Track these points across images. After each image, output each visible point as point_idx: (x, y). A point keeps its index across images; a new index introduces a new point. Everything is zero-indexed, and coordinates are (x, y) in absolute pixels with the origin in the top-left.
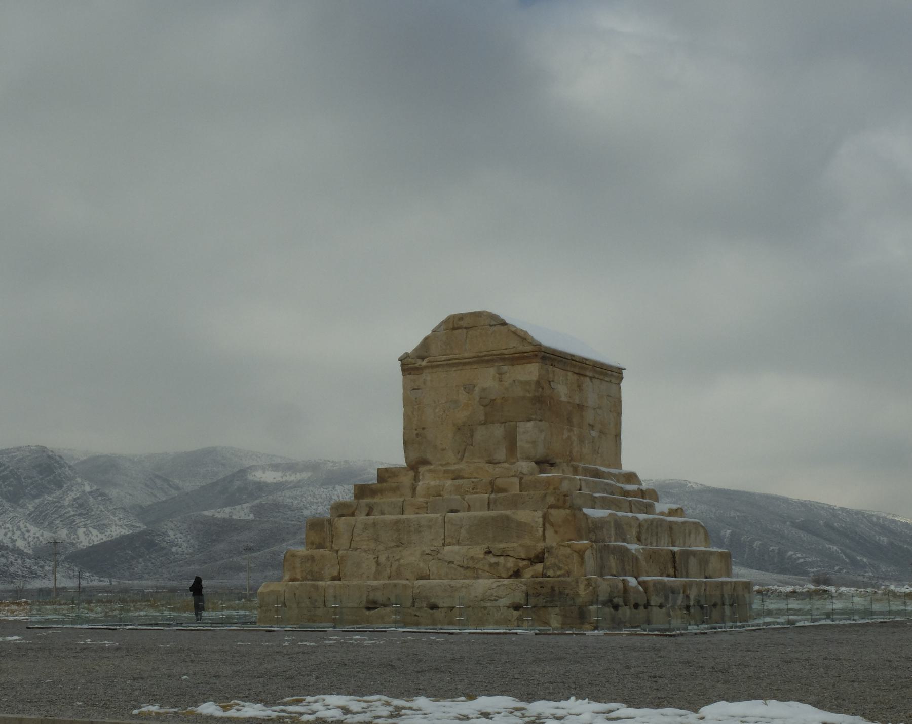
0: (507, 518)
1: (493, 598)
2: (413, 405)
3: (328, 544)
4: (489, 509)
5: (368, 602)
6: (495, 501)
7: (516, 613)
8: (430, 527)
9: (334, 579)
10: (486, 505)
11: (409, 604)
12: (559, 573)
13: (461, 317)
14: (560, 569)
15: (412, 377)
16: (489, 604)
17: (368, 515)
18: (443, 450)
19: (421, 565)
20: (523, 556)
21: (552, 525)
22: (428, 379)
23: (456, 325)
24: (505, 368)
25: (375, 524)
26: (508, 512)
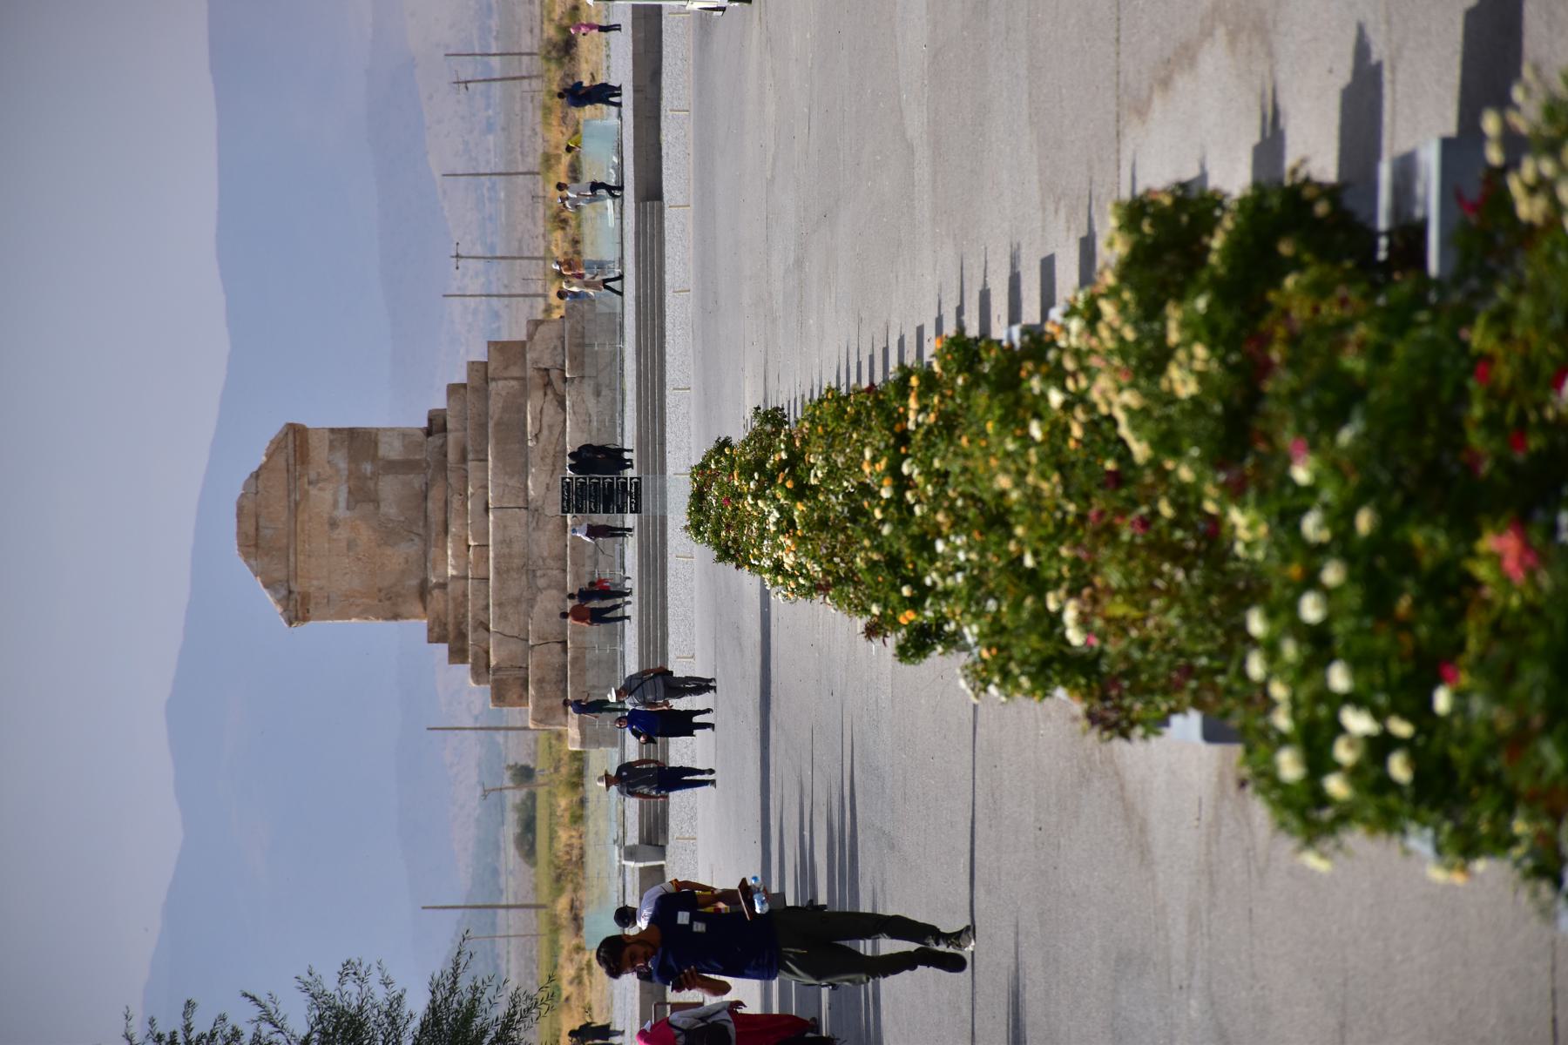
0: (497, 424)
2: (345, 607)
7: (605, 392)
9: (565, 650)
13: (241, 534)
15: (312, 607)
19: (550, 527)
21: (506, 368)
22: (315, 582)
23: (253, 543)
24: (313, 476)
25: (500, 605)
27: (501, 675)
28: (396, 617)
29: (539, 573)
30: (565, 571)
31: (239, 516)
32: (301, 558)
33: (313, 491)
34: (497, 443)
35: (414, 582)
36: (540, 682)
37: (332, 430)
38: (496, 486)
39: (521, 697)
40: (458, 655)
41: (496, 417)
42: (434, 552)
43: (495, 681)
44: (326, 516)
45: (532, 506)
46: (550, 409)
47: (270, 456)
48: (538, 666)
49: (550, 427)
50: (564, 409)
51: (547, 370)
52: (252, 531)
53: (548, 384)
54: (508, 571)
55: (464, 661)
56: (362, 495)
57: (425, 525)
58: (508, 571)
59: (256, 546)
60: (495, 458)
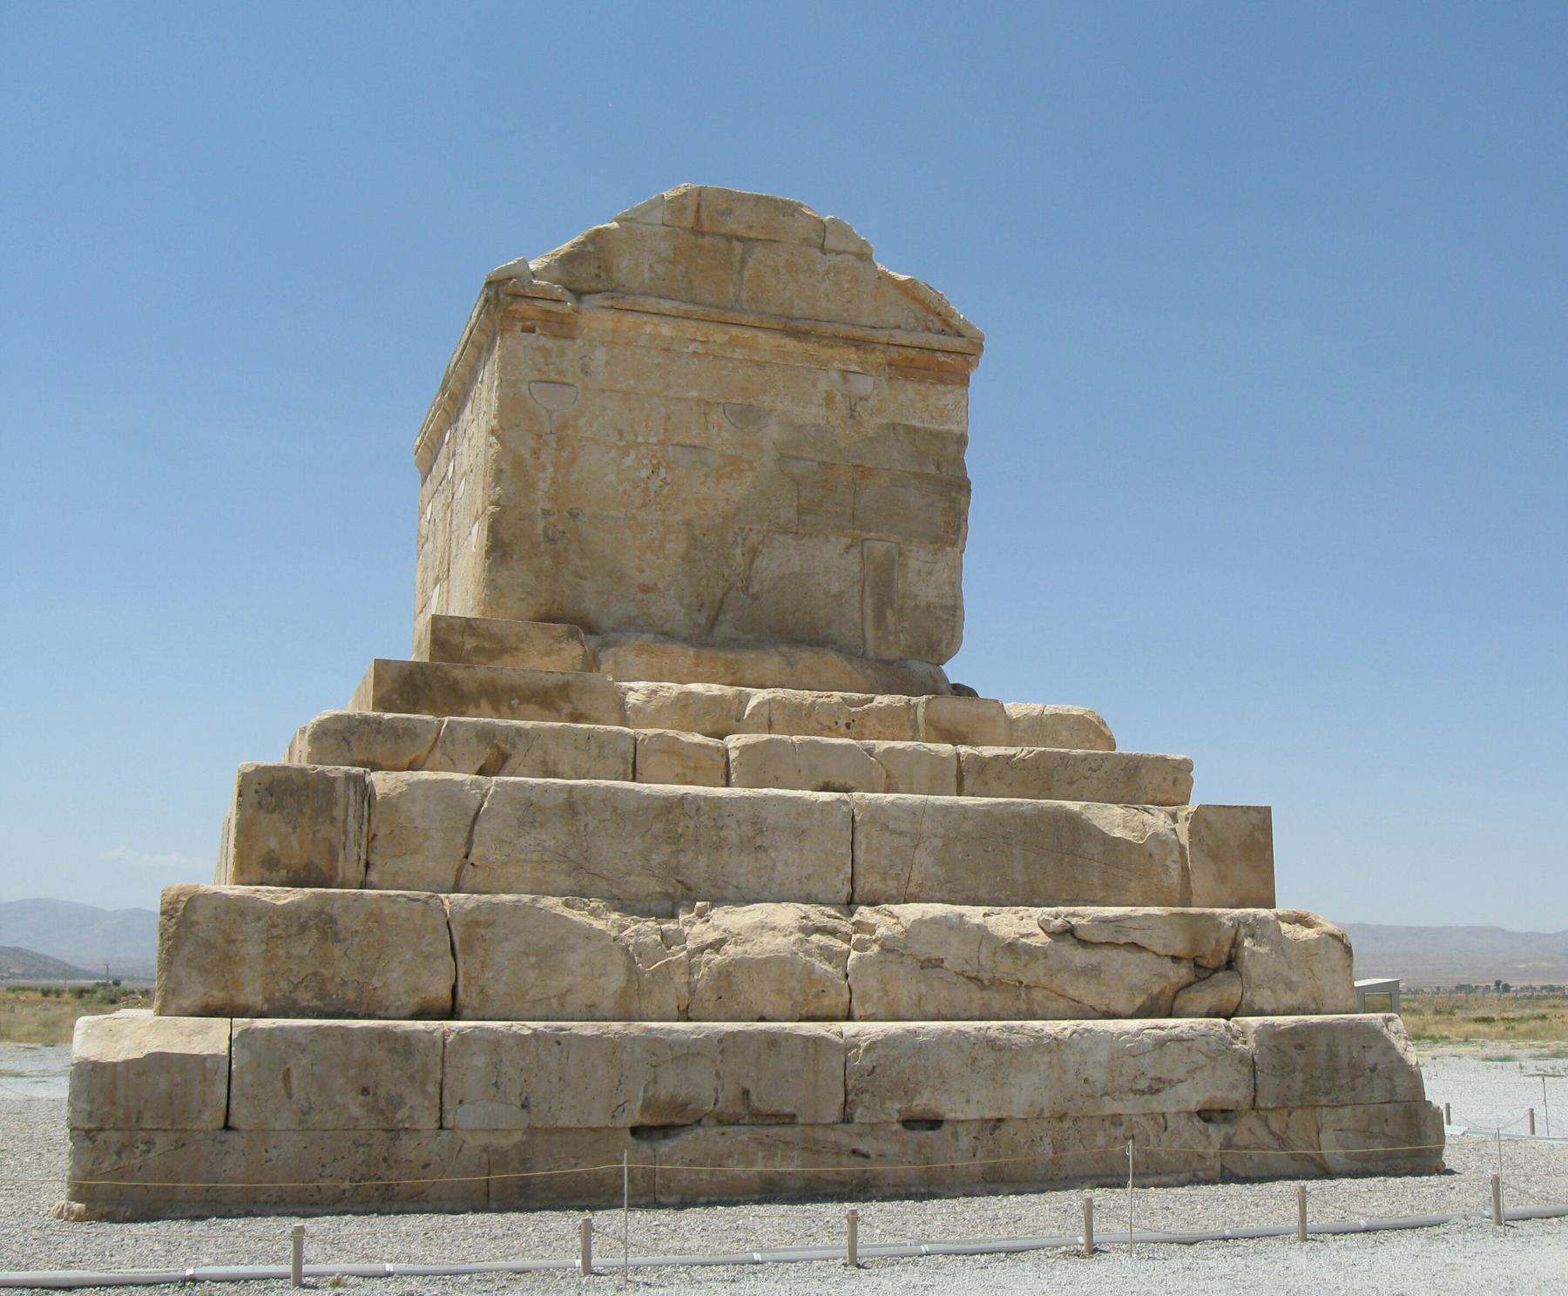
0: (1073, 820)
1: (1143, 1084)
3: (349, 867)
5: (645, 1108)
6: (982, 764)
7: (1217, 1133)
8: (801, 835)
10: (953, 781)
11: (833, 1112)
12: (1288, 999)
14: (1290, 986)
16: (1128, 1106)
17: (480, 772)
18: (646, 589)
20: (1180, 947)
22: (601, 355)
25: (572, 806)
26: (1074, 806)
27: (347, 801)
31: (767, 199)
32: (666, 330)
36: (324, 924)
37: (962, 440)
40: (403, 686)
43: (329, 782)
46: (1142, 974)
47: (908, 290)
48: (375, 916)
50: (1208, 1015)
51: (1231, 964)
54: (674, 838)
55: (382, 703)
60: (988, 812)
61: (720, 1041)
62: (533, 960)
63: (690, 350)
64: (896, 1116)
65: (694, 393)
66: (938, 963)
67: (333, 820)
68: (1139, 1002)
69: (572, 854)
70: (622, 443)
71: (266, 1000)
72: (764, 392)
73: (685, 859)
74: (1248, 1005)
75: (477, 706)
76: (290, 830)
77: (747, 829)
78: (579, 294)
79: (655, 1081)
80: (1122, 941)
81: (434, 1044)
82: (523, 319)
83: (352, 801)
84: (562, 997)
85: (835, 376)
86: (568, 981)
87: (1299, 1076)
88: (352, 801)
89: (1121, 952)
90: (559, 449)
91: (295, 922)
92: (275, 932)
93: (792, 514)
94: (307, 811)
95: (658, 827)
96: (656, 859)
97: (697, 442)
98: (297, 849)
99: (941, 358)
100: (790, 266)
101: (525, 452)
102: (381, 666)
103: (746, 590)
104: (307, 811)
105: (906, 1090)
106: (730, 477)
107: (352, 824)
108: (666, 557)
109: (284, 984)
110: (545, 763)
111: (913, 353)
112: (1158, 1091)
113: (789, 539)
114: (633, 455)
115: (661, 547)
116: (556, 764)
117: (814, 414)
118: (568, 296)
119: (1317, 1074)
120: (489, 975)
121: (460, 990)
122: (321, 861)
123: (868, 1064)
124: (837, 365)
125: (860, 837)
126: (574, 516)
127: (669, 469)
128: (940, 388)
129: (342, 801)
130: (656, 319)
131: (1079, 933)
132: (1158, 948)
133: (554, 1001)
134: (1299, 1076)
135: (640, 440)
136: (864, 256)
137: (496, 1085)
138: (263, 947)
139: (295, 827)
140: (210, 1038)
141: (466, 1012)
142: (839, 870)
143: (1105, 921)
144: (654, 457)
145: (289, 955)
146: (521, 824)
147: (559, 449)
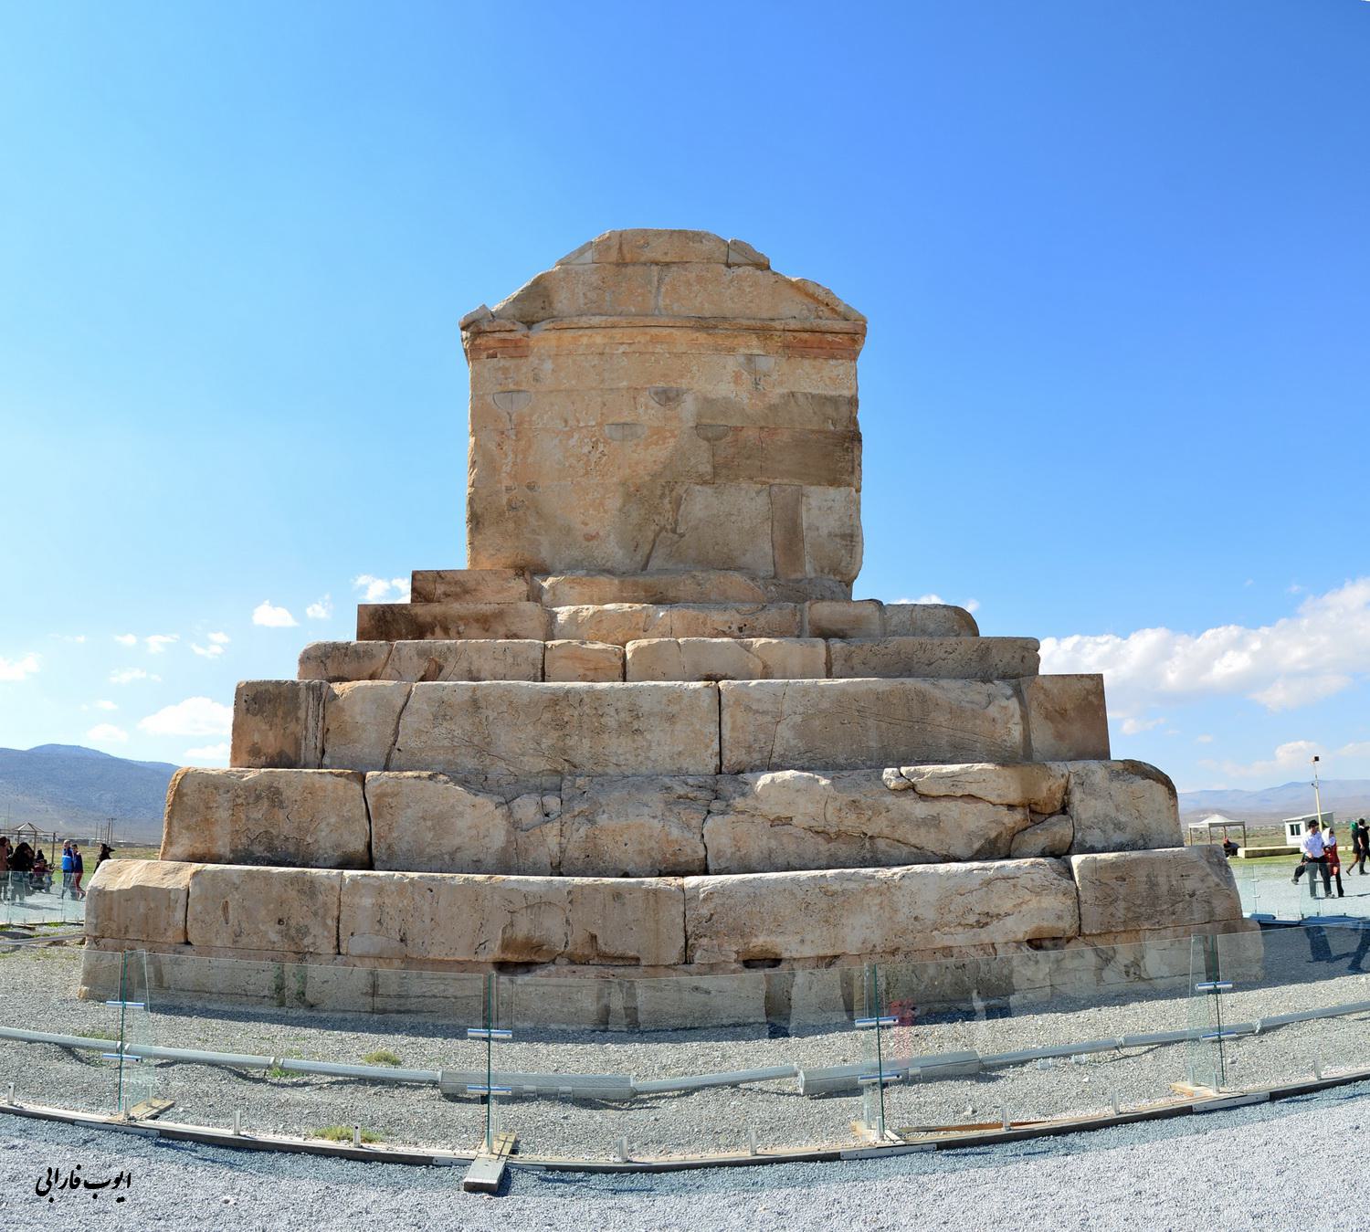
0: (923, 698)
1: (972, 919)
4: (829, 675)
8: (671, 718)
9: (345, 864)
12: (1117, 838)
15: (501, 362)
18: (589, 538)
19: (675, 833)
24: (765, 364)
25: (475, 704)
27: (307, 706)
28: (476, 521)
29: (552, 802)
30: (557, 870)
32: (599, 339)
33: (732, 364)
34: (879, 697)
35: (545, 554)
37: (853, 402)
38: (777, 697)
39: (255, 751)
40: (379, 622)
41: (937, 693)
42: (610, 584)
44: (684, 384)
45: (726, 786)
46: (977, 821)
47: (800, 288)
48: (311, 790)
49: (934, 822)
51: (1064, 809)
52: (648, 254)
53: (1035, 812)
54: (561, 725)
55: (361, 635)
56: (729, 450)
57: (659, 566)
58: (561, 725)
59: (621, 264)
60: (843, 691)
61: (569, 893)
62: (429, 823)
63: (620, 351)
64: (734, 956)
65: (625, 383)
66: (788, 821)
67: (297, 719)
68: (977, 846)
69: (476, 740)
70: (568, 429)
71: (232, 851)
72: (682, 376)
73: (570, 742)
74: (1080, 844)
75: (433, 633)
76: (268, 728)
77: (624, 716)
78: (530, 324)
79: (512, 925)
80: (959, 794)
81: (333, 888)
82: (487, 349)
83: (311, 705)
84: (452, 854)
85: (742, 359)
86: (457, 841)
87: (1121, 905)
88: (311, 705)
89: (960, 803)
90: (518, 440)
91: (254, 794)
92: (239, 801)
93: (709, 468)
94: (280, 713)
95: (547, 716)
96: (546, 742)
97: (628, 420)
98: (271, 741)
99: (829, 337)
100: (700, 279)
101: (492, 446)
102: (363, 609)
103: (674, 531)
104: (280, 713)
105: (739, 931)
106: (657, 444)
107: (311, 723)
108: (606, 512)
109: (244, 840)
110: (470, 671)
111: (806, 336)
112: (987, 924)
113: (708, 490)
114: (576, 436)
115: (602, 504)
116: (479, 671)
117: (724, 389)
118: (519, 326)
119: (1139, 902)
120: (395, 835)
121: (373, 847)
122: (290, 751)
123: (705, 911)
124: (743, 350)
125: (726, 717)
126: (531, 487)
127: (605, 442)
128: (832, 362)
129: (303, 706)
130: (588, 332)
131: (919, 788)
132: (993, 799)
133: (446, 857)
134: (1121, 905)
135: (582, 424)
136: (763, 266)
137: (379, 921)
138: (231, 812)
139: (271, 726)
140: (182, 876)
141: (376, 864)
142: (707, 747)
143: (943, 777)
144: (593, 436)
145: (248, 818)
146: (435, 718)
147: (518, 440)
